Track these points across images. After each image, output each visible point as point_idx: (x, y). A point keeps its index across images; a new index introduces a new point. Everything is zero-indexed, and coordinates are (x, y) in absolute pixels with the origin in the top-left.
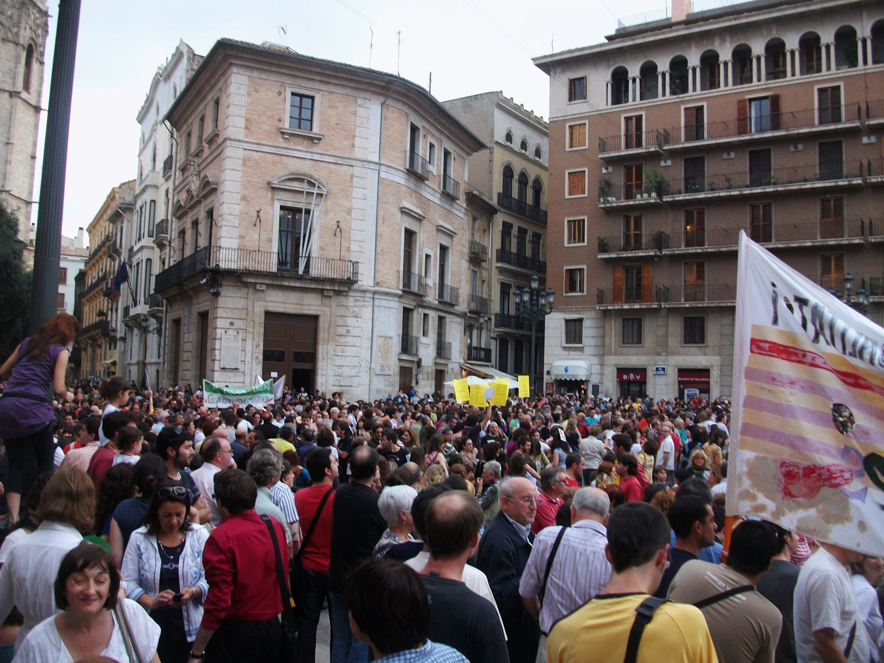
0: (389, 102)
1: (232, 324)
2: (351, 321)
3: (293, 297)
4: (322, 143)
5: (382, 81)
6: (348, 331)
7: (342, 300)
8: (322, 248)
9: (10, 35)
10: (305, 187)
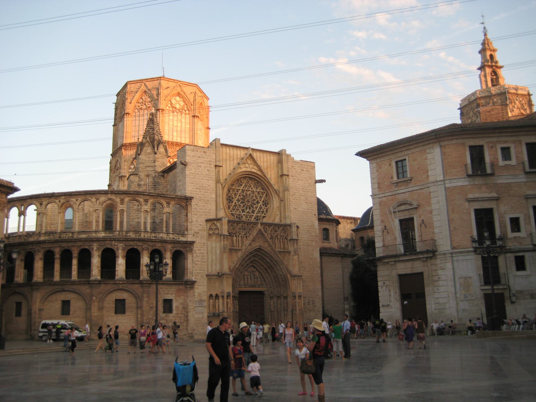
0: (442, 144)
1: (384, 283)
2: (440, 272)
3: (409, 264)
4: (412, 181)
5: (433, 136)
6: (439, 278)
7: (433, 261)
8: (421, 236)
10: (408, 207)
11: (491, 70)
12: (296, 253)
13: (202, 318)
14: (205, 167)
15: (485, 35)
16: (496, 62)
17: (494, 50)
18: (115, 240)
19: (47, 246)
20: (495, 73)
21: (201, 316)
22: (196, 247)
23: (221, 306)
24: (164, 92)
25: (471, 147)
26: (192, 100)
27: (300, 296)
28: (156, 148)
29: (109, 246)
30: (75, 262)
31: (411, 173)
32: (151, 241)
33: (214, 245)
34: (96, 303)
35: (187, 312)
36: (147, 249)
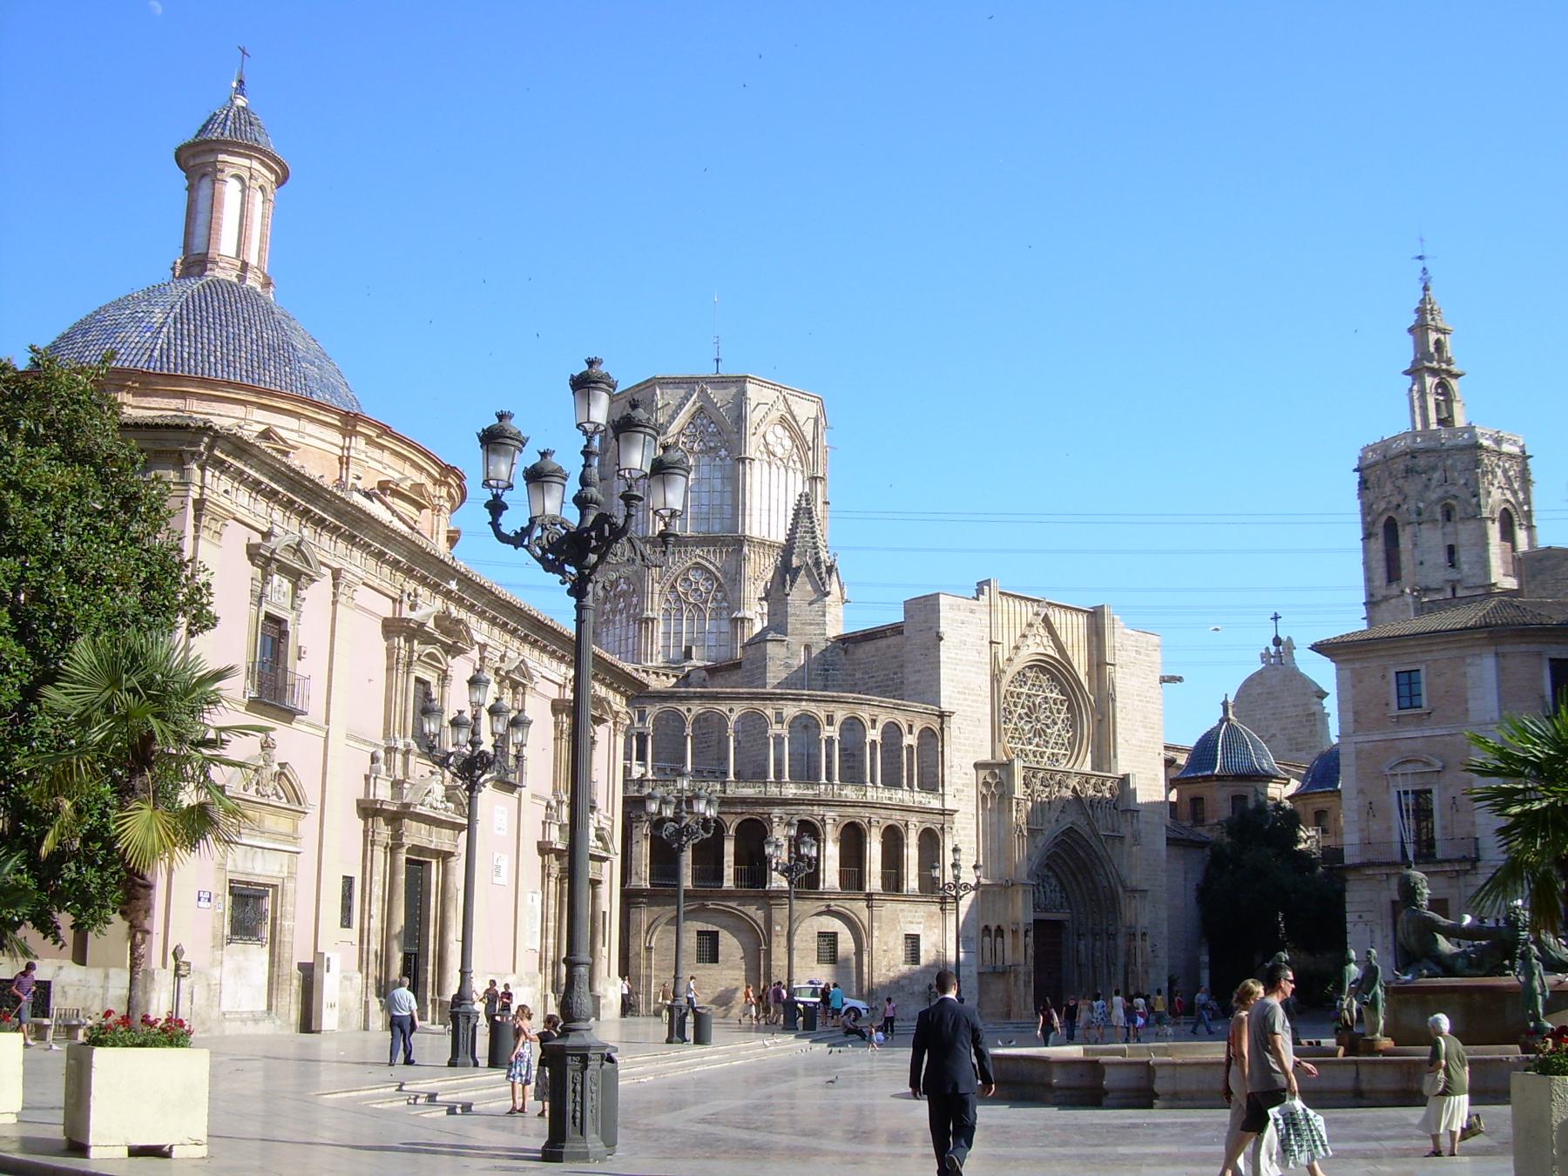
0: (1501, 649)
8: (1444, 828)
9: (1470, 510)
10: (1420, 768)
11: (1436, 381)
12: (1136, 839)
15: (1426, 289)
16: (1449, 362)
17: (1444, 332)
18: (821, 803)
20: (1443, 388)
23: (1008, 953)
24: (753, 417)
25: (1551, 660)
26: (809, 438)
27: (1144, 934)
30: (729, 847)
31: (1429, 701)
32: (885, 807)
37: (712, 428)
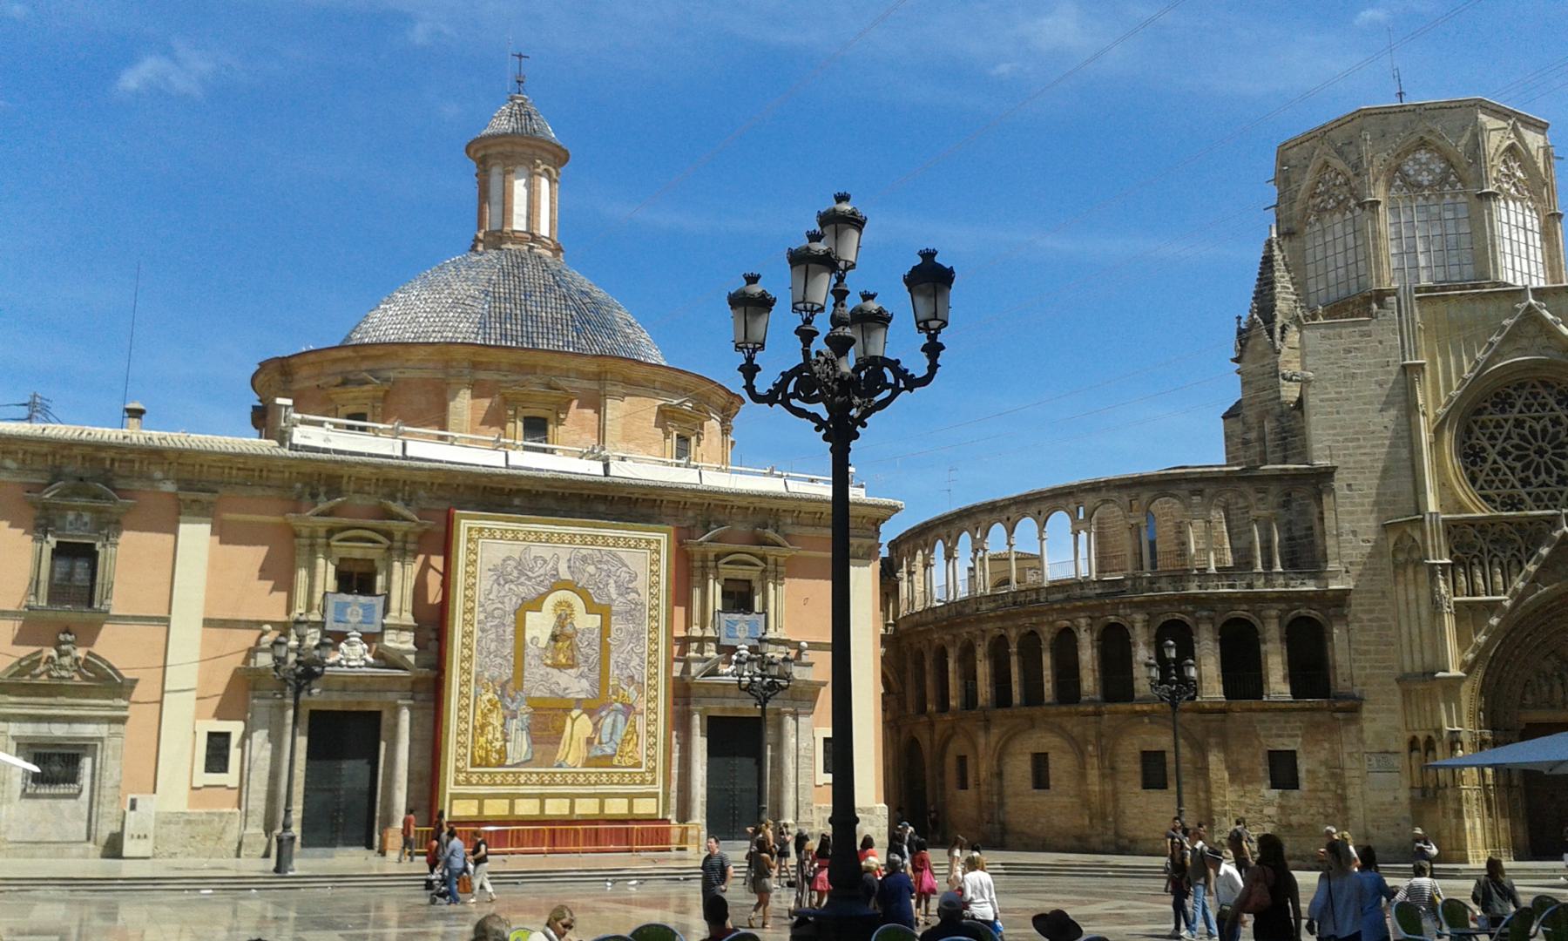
13: (1392, 804)
14: (1369, 375)
19: (994, 629)
21: (1389, 797)
22: (1356, 607)
28: (1277, 335)
29: (1112, 619)
30: (1047, 660)
33: (1412, 596)
34: (1095, 760)
35: (1344, 788)
36: (1211, 620)
37: (1340, 179)
